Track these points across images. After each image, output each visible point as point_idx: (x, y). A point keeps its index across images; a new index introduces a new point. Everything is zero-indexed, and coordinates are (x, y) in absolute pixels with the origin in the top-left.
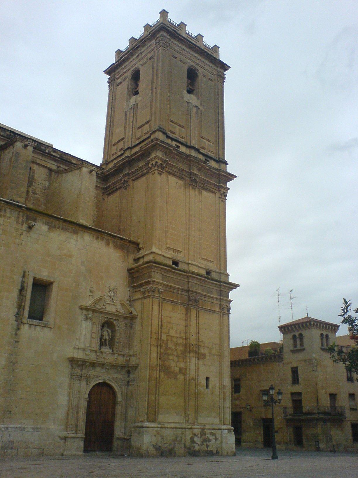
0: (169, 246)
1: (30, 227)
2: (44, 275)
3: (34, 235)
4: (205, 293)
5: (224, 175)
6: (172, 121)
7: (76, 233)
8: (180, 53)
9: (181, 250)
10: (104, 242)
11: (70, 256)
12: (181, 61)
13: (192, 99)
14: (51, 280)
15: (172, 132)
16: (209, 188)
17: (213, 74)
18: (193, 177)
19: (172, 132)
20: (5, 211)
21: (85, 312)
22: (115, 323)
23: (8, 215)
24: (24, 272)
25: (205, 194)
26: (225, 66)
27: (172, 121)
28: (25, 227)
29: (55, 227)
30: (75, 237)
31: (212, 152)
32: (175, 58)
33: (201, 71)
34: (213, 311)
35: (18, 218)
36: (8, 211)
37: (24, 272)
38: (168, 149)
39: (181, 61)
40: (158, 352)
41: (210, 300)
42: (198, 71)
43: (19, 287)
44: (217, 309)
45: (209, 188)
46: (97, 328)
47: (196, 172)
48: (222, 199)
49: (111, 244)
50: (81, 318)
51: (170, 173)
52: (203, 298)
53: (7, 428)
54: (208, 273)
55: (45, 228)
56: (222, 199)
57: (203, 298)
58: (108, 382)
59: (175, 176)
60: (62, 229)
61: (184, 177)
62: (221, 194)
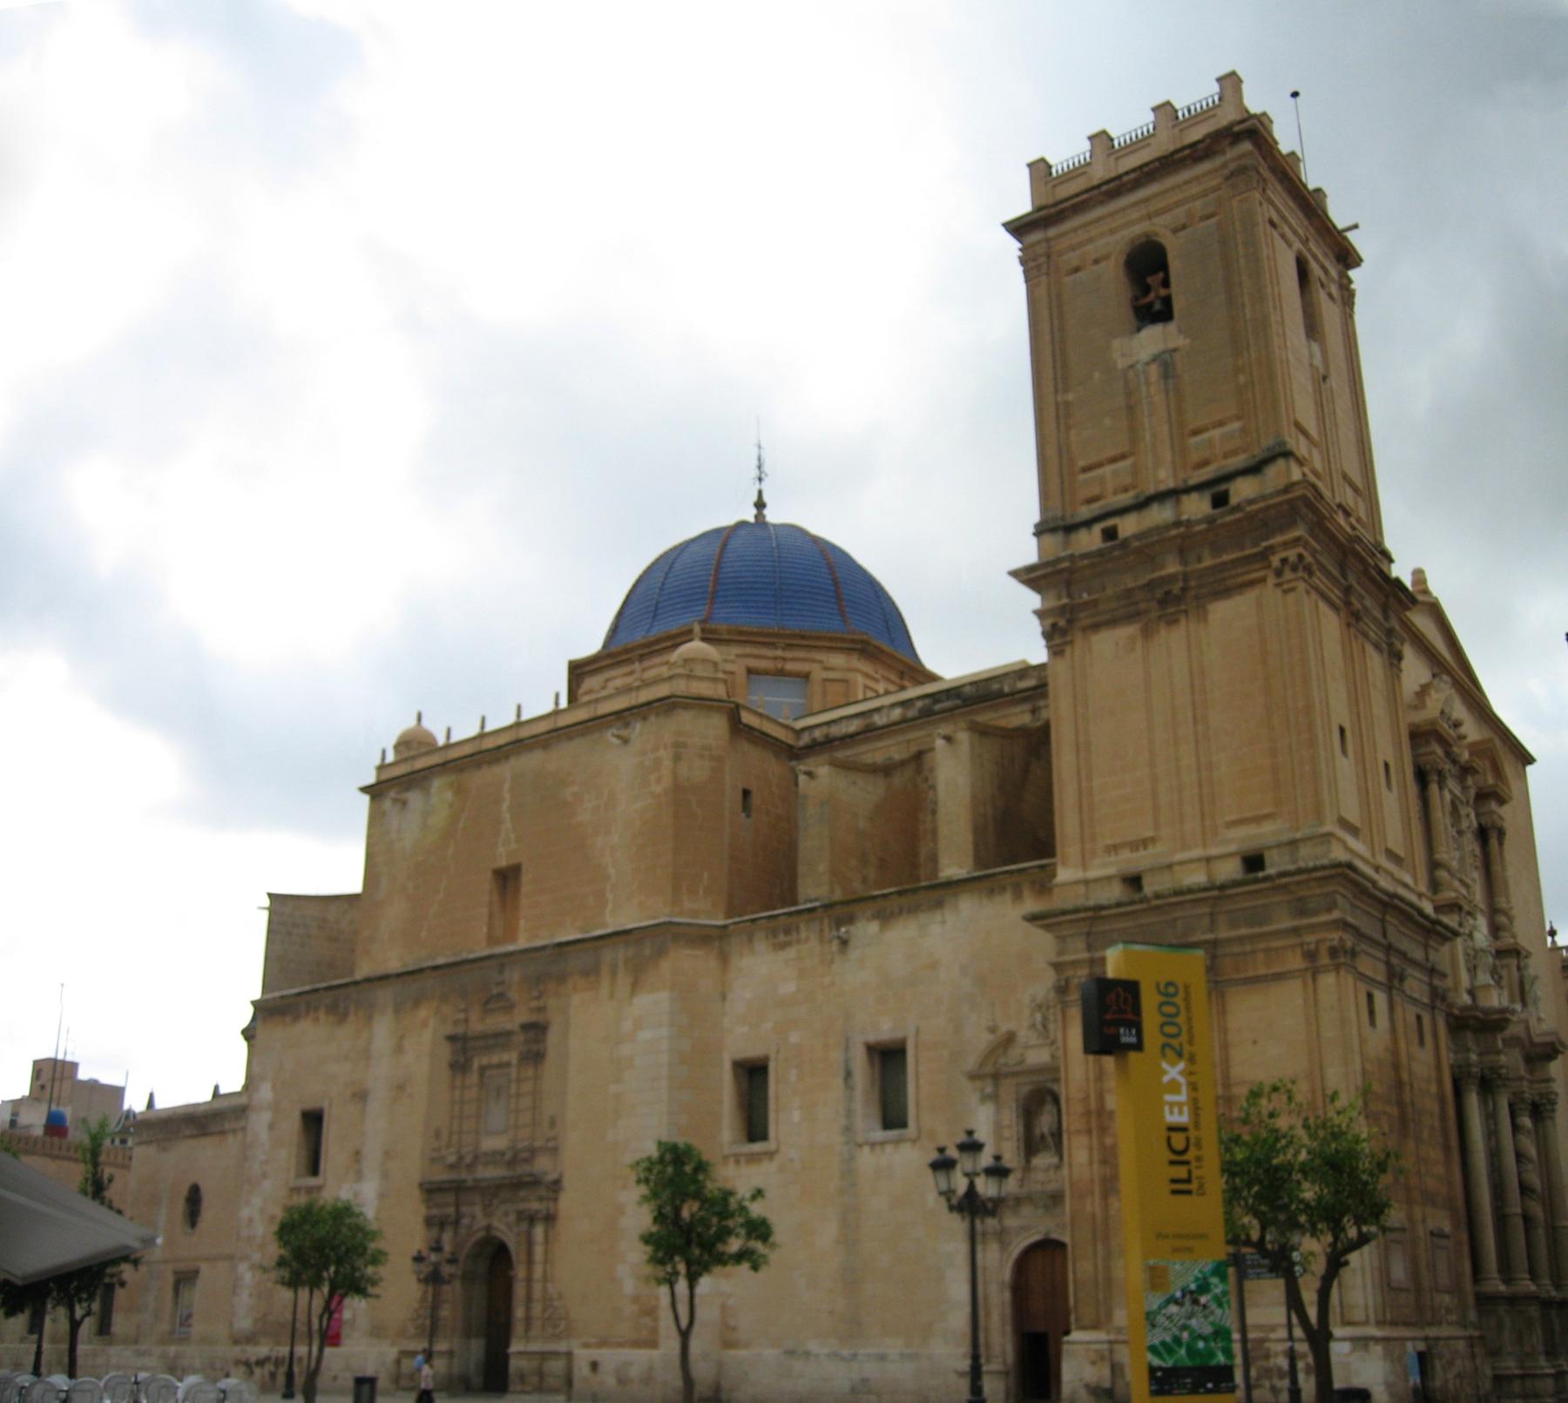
0: (1109, 842)
1: (844, 943)
2: (885, 1031)
3: (854, 953)
4: (1244, 931)
5: (1268, 508)
6: (1085, 470)
7: (939, 905)
8: (1091, 240)
9: (1150, 834)
10: (1008, 896)
11: (934, 965)
12: (1096, 262)
13: (1152, 339)
14: (899, 1035)
15: (1090, 501)
16: (1233, 581)
17: (1215, 189)
18: (1159, 593)
19: (1090, 501)
20: (798, 930)
21: (979, 1084)
22: (1055, 1087)
23: (803, 935)
24: (847, 1040)
25: (1220, 610)
26: (1236, 129)
27: (1085, 470)
28: (835, 946)
29: (892, 915)
30: (938, 916)
31: (1234, 453)
32: (1077, 270)
33: (1160, 228)
34: (1279, 977)
35: (822, 931)
36: (802, 926)
37: (847, 1040)
38: (1060, 572)
39: (1096, 262)
40: (1091, 1149)
41: (1261, 945)
42: (1156, 234)
43: (842, 1074)
44: (1296, 962)
45: (1233, 581)
46: (1010, 1116)
47: (1172, 567)
48: (1286, 586)
49: (1027, 893)
50: (974, 1099)
51: (1096, 627)
52: (1236, 949)
53: (855, 1355)
54: (1253, 862)
55: (874, 927)
56: (1286, 586)
57: (1236, 949)
58: (1054, 1236)
59: (1113, 622)
60: (909, 911)
61: (1142, 606)
62: (1279, 573)
